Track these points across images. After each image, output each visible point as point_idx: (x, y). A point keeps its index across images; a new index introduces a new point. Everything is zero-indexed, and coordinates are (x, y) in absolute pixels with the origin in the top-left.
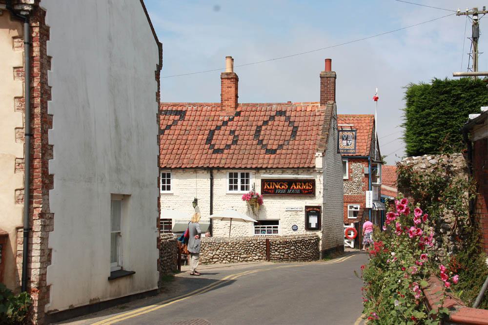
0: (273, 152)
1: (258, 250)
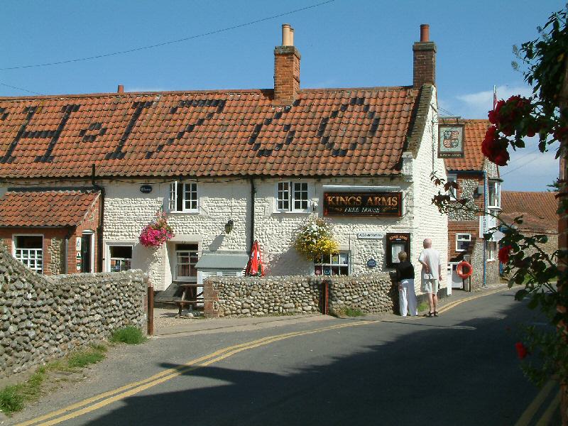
0: (344, 153)
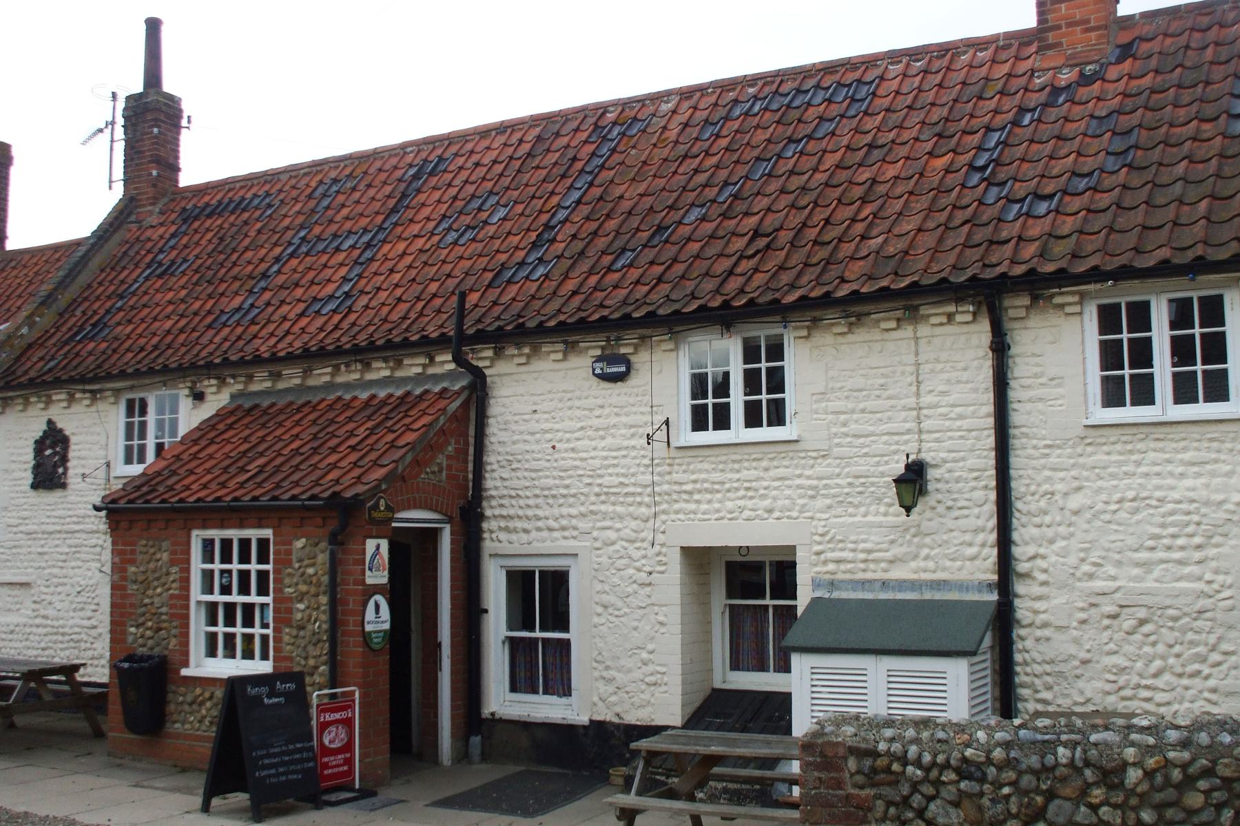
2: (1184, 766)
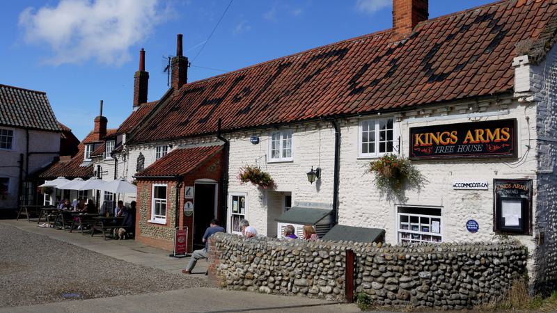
1: (330, 272)
2: (285, 251)
